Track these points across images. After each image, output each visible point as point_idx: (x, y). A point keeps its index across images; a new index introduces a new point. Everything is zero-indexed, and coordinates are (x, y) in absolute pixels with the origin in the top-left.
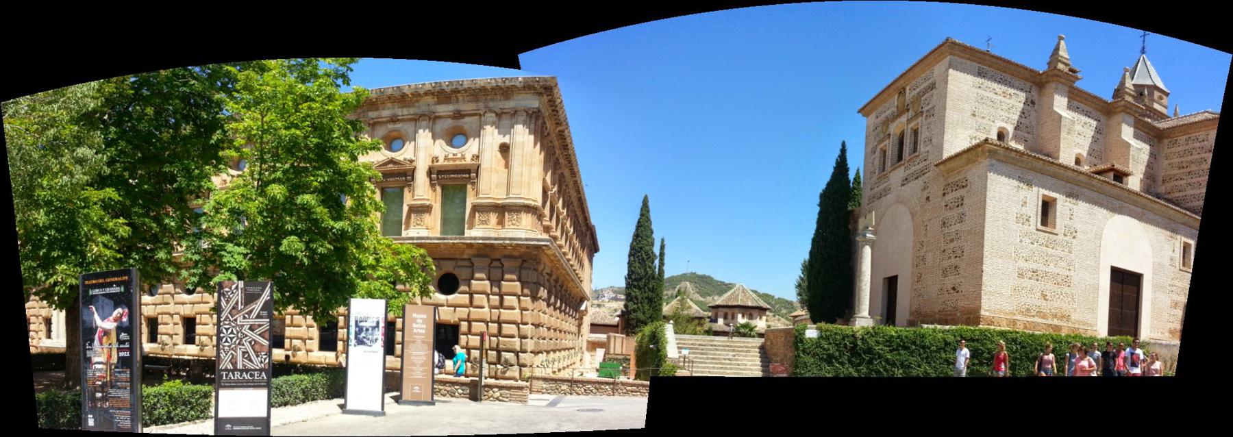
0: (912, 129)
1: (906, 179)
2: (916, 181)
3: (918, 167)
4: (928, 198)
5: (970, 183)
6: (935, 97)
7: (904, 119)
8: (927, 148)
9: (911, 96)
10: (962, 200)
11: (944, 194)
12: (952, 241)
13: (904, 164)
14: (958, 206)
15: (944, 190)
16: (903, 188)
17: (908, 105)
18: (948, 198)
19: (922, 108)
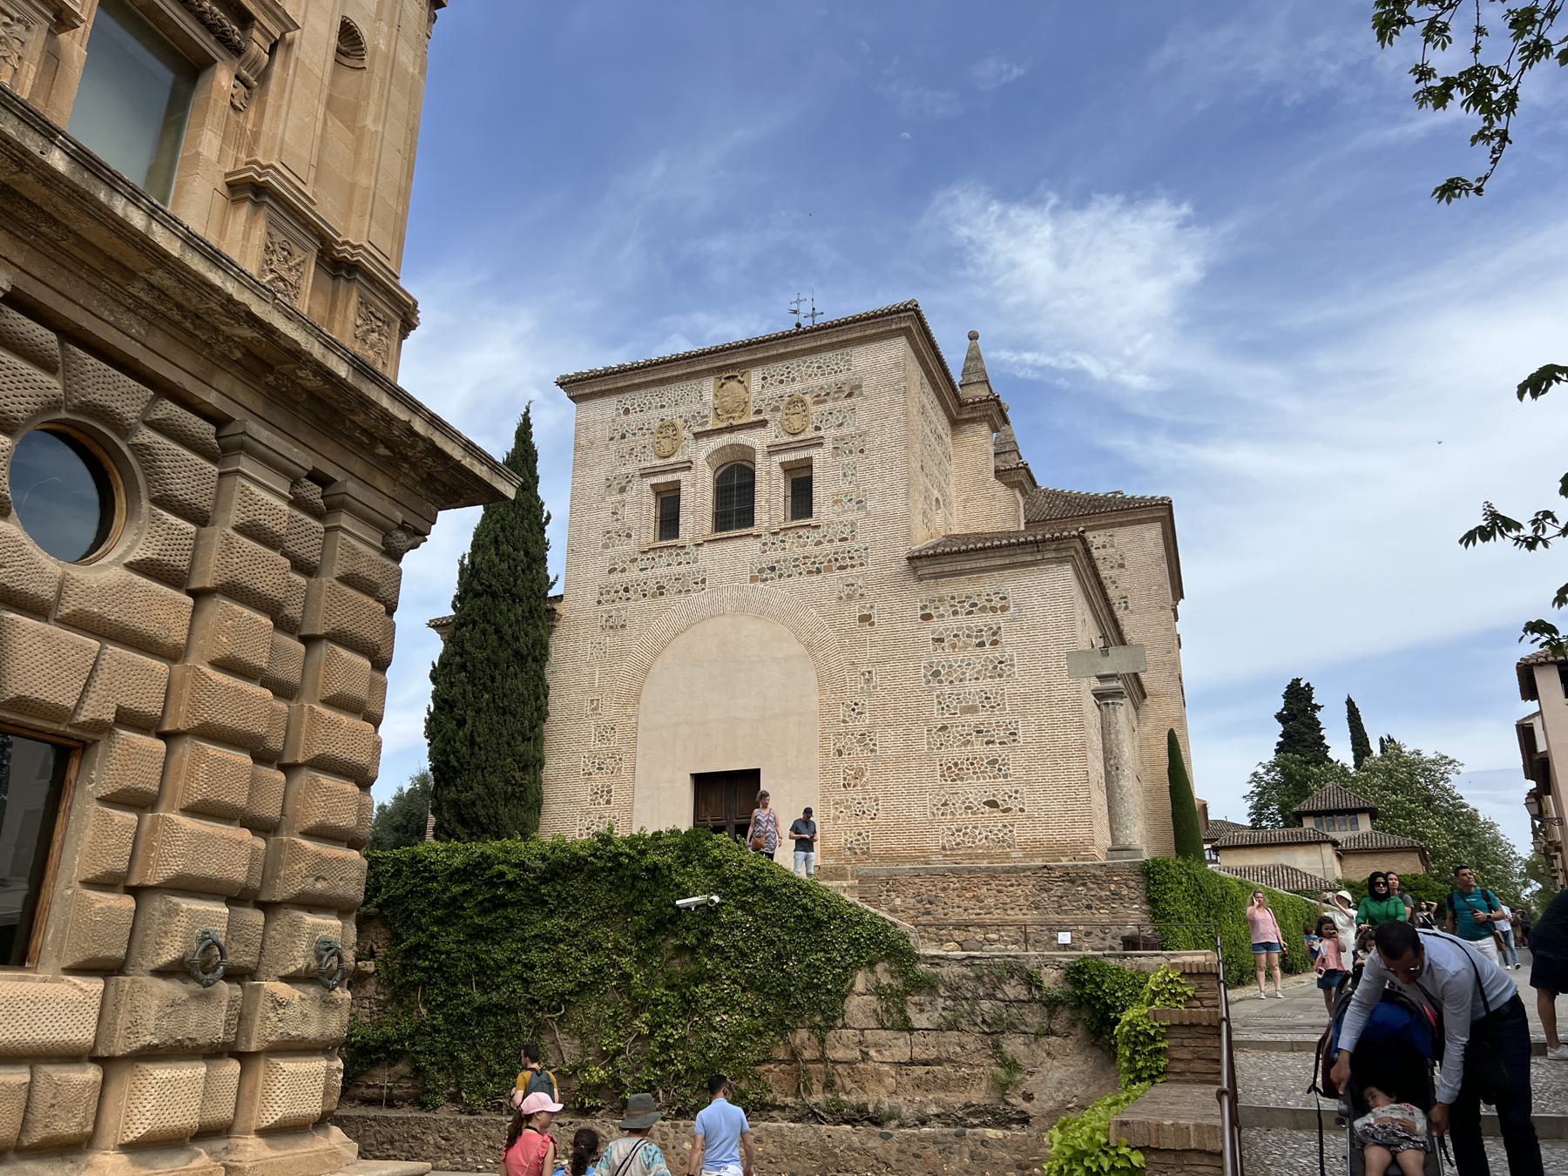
0: (782, 464)
1: (773, 569)
2: (814, 578)
3: (811, 549)
4: (866, 619)
5: (1016, 605)
6: (863, 416)
7: (756, 440)
8: (850, 517)
9: (768, 393)
10: (994, 634)
11: (927, 617)
12: (972, 710)
13: (759, 536)
14: (982, 644)
15: (924, 608)
16: (761, 585)
17: (759, 412)
18: (935, 623)
19: (818, 429)
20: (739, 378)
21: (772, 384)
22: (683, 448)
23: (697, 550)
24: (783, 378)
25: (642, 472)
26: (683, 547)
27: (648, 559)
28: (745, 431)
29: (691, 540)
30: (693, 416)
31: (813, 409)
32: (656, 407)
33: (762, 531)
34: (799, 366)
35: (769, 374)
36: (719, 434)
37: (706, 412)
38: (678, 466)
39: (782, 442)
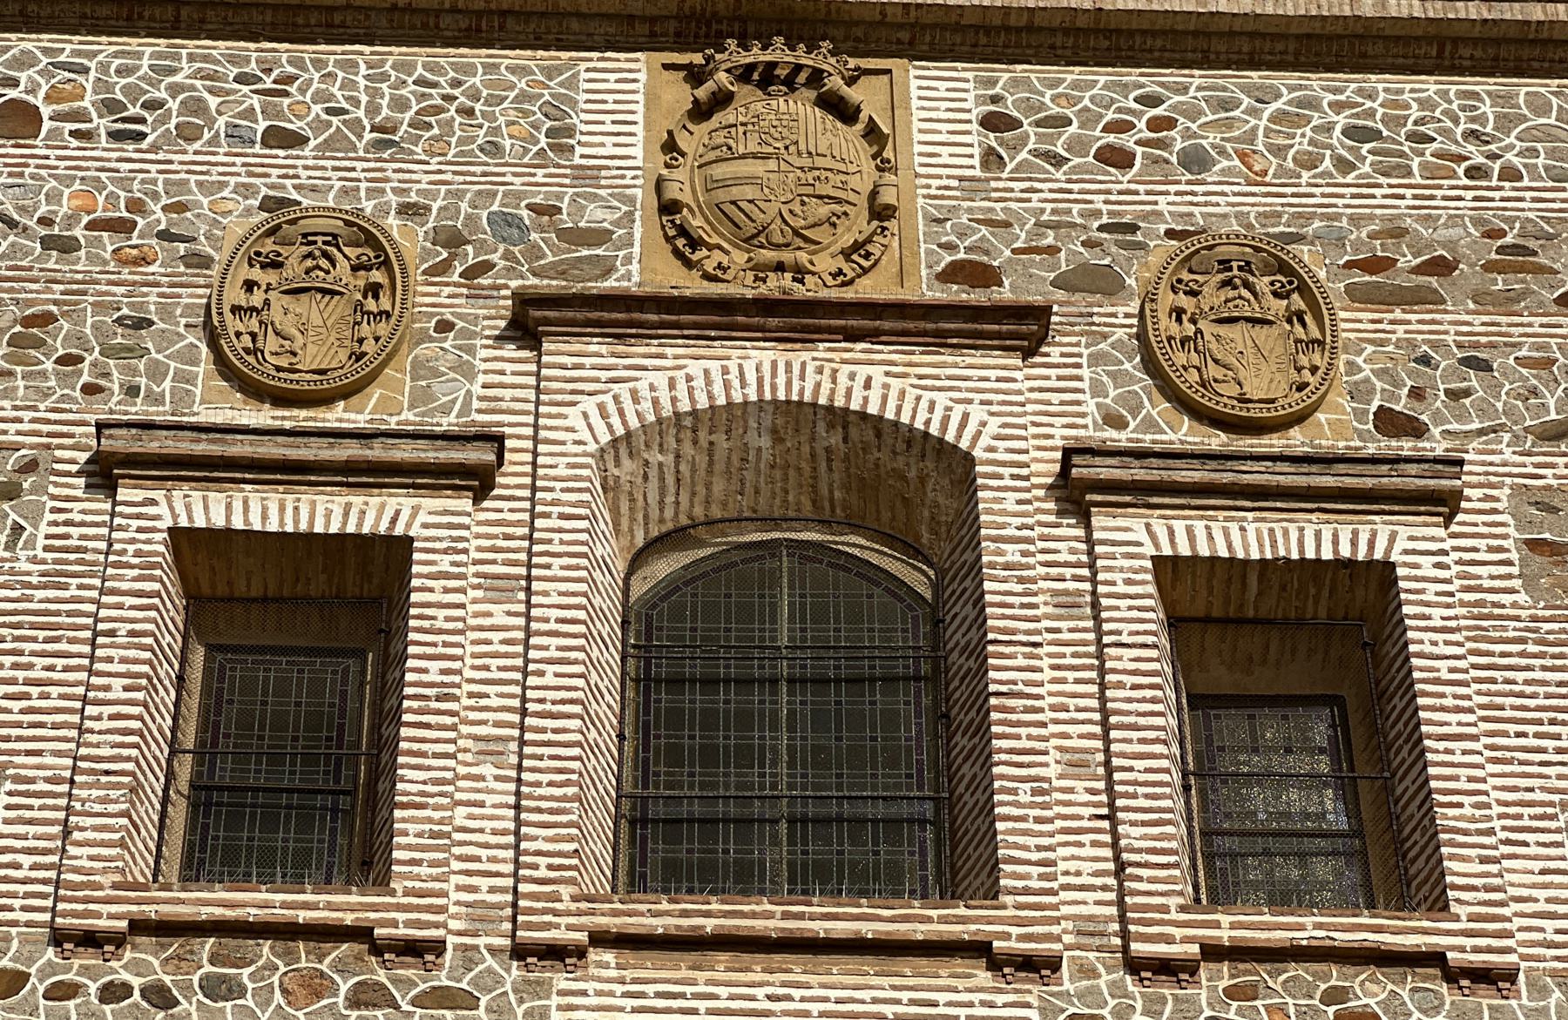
0: (1168, 570)
20: (835, 82)
21: (1058, 161)
22: (422, 369)
23: (540, 989)
24: (1127, 141)
25: (119, 442)
26: (413, 949)
27: (113, 992)
28: (886, 352)
29: (480, 916)
30: (505, 223)
31: (1353, 322)
32: (234, 134)
33: (1062, 940)
34: (1227, 105)
35: (1030, 107)
36: (701, 333)
37: (596, 215)
38: (405, 452)
39: (1148, 440)
